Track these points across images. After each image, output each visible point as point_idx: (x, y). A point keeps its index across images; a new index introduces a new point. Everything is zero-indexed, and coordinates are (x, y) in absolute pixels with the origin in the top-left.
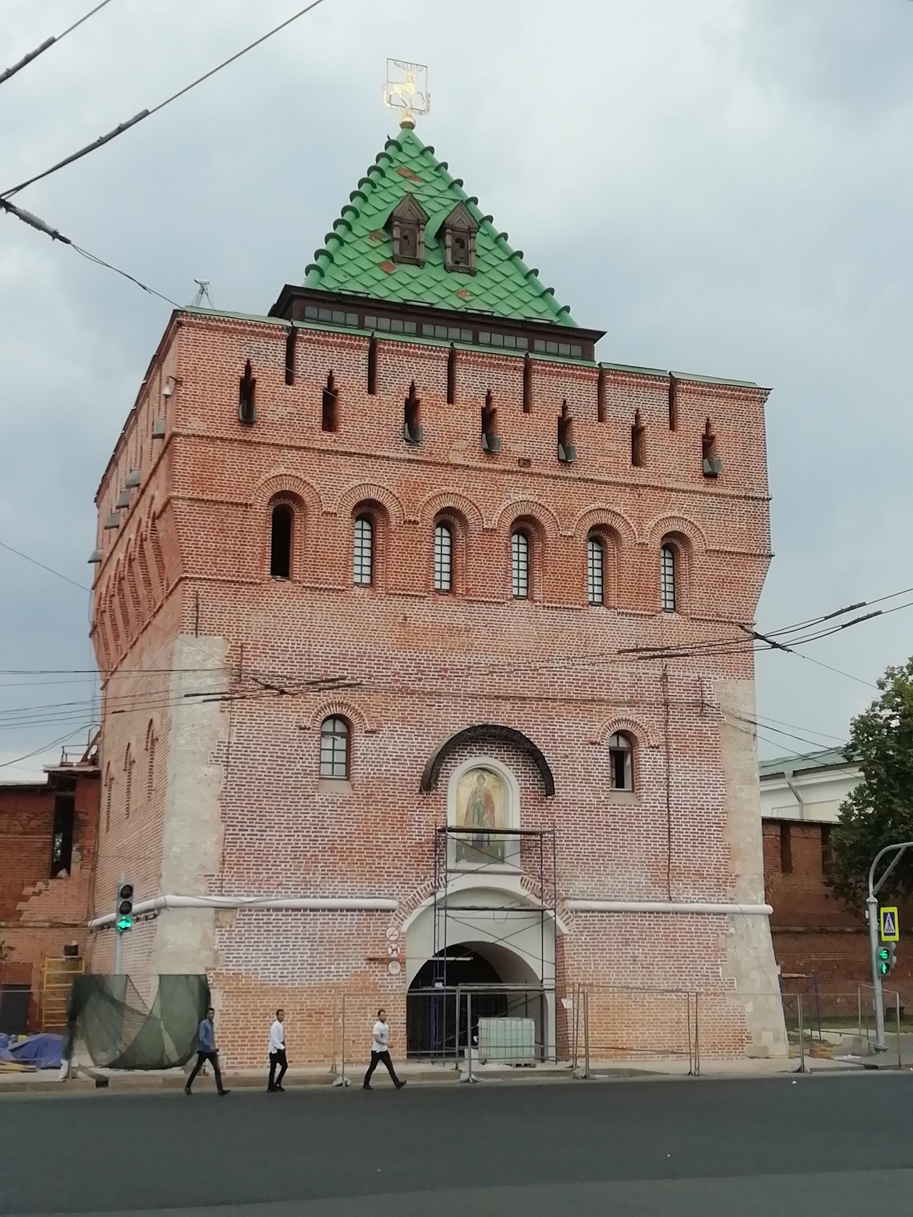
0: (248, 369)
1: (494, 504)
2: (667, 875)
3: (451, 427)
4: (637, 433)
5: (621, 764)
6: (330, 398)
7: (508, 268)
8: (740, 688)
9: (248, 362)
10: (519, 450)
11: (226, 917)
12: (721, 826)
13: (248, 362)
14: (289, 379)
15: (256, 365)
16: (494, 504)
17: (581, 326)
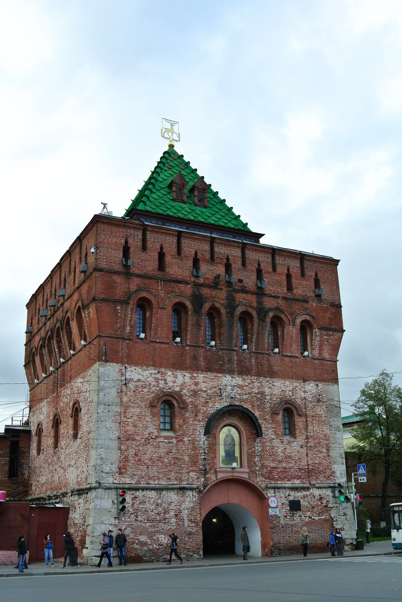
0: (126, 242)
7: (219, 206)
9: (126, 239)
13: (126, 239)
15: (130, 241)
17: (253, 231)
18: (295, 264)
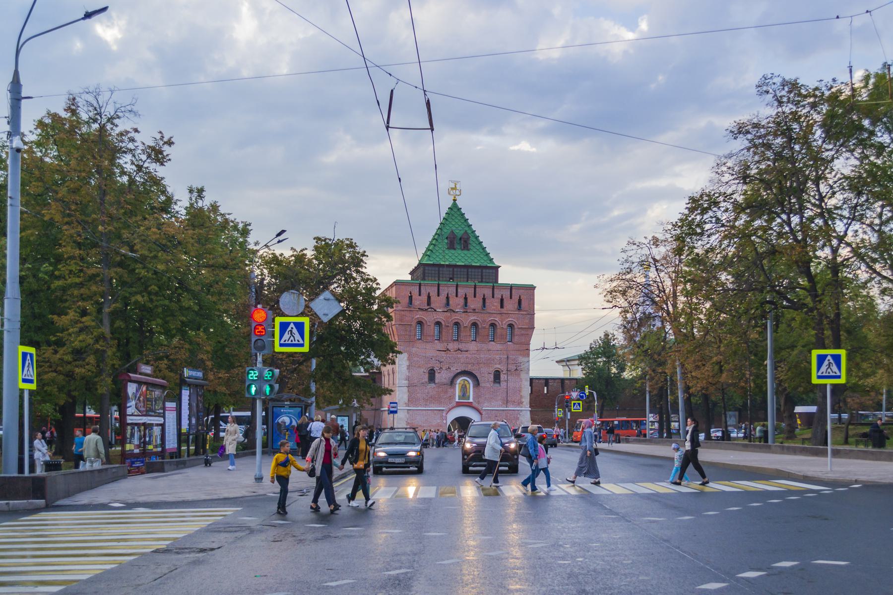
1: (467, 320)
2: (507, 402)
3: (457, 303)
4: (502, 300)
5: (497, 376)
6: (429, 297)
8: (525, 359)
10: (472, 307)
11: (411, 412)
12: (520, 391)
14: (420, 295)
16: (467, 320)
18: (506, 293)
